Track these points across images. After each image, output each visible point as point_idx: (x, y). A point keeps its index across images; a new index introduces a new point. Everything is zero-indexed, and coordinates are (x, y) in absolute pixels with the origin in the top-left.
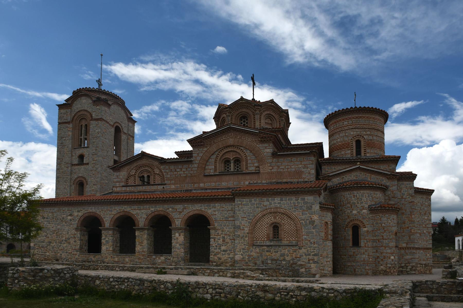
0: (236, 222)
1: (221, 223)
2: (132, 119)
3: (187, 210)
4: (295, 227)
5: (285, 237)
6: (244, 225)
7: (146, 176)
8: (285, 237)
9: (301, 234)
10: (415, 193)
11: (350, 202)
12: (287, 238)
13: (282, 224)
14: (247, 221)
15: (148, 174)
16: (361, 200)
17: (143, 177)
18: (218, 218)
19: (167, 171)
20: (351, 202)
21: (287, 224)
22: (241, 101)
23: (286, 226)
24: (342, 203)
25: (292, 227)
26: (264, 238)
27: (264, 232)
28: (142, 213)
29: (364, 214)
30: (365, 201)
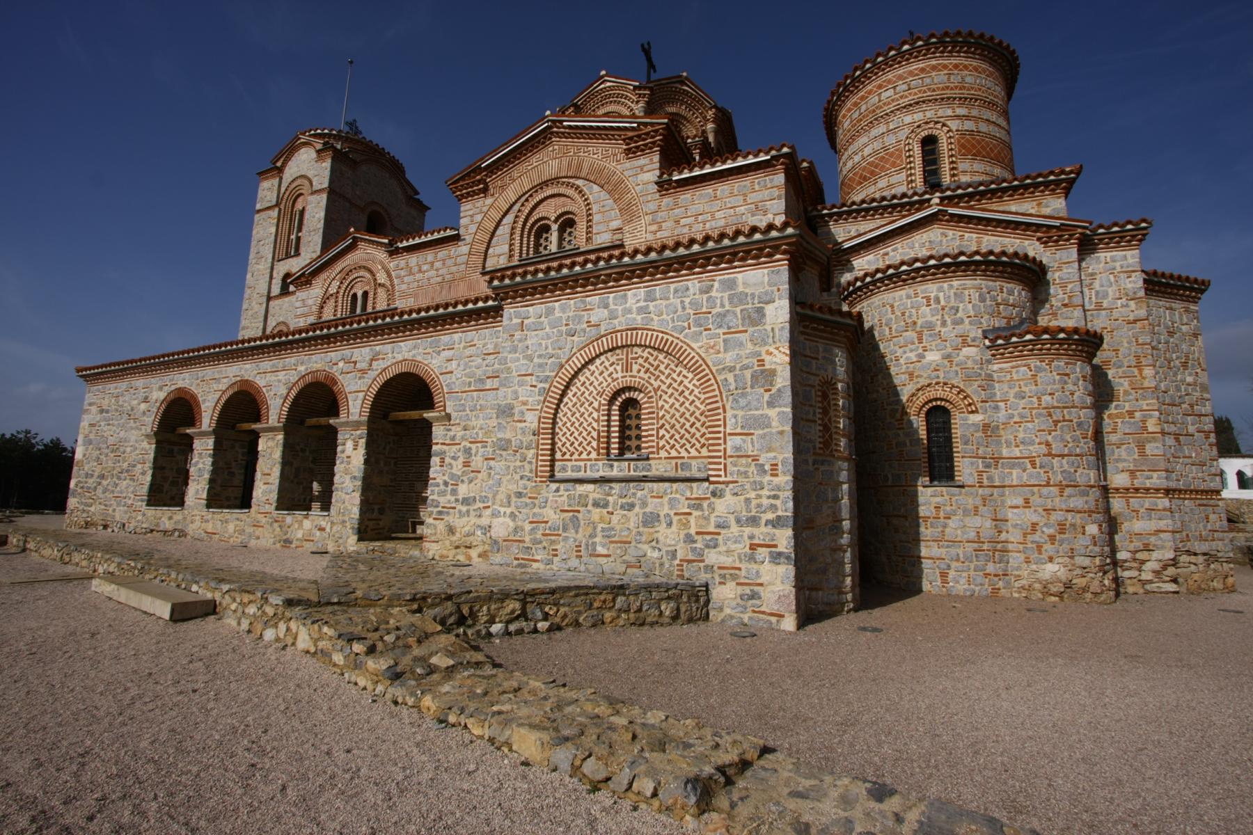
0: (501, 393)
1: (463, 402)
2: (419, 202)
3: (381, 361)
4: (697, 403)
5: (662, 443)
6: (524, 403)
7: (360, 294)
8: (662, 443)
9: (721, 429)
10: (1146, 289)
11: (915, 323)
12: (668, 447)
13: (653, 393)
14: (535, 386)
15: (366, 288)
16: (954, 311)
17: (355, 296)
18: (457, 383)
19: (403, 273)
20: (919, 322)
21: (670, 391)
22: (602, 86)
23: (665, 401)
24: (887, 329)
25: (687, 404)
26: (589, 449)
27: (589, 429)
28: (279, 381)
29: (970, 364)
30: (972, 313)
